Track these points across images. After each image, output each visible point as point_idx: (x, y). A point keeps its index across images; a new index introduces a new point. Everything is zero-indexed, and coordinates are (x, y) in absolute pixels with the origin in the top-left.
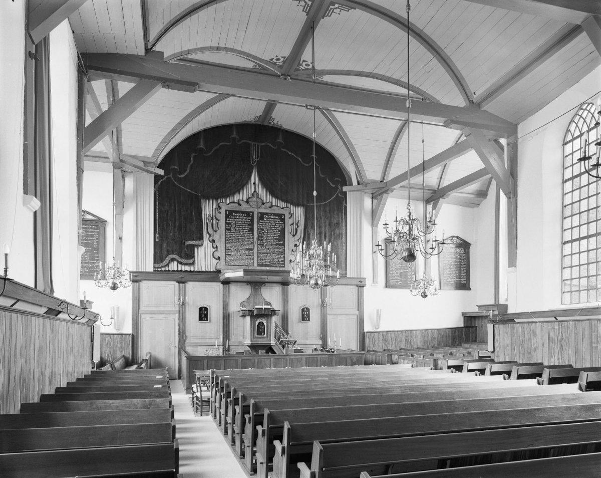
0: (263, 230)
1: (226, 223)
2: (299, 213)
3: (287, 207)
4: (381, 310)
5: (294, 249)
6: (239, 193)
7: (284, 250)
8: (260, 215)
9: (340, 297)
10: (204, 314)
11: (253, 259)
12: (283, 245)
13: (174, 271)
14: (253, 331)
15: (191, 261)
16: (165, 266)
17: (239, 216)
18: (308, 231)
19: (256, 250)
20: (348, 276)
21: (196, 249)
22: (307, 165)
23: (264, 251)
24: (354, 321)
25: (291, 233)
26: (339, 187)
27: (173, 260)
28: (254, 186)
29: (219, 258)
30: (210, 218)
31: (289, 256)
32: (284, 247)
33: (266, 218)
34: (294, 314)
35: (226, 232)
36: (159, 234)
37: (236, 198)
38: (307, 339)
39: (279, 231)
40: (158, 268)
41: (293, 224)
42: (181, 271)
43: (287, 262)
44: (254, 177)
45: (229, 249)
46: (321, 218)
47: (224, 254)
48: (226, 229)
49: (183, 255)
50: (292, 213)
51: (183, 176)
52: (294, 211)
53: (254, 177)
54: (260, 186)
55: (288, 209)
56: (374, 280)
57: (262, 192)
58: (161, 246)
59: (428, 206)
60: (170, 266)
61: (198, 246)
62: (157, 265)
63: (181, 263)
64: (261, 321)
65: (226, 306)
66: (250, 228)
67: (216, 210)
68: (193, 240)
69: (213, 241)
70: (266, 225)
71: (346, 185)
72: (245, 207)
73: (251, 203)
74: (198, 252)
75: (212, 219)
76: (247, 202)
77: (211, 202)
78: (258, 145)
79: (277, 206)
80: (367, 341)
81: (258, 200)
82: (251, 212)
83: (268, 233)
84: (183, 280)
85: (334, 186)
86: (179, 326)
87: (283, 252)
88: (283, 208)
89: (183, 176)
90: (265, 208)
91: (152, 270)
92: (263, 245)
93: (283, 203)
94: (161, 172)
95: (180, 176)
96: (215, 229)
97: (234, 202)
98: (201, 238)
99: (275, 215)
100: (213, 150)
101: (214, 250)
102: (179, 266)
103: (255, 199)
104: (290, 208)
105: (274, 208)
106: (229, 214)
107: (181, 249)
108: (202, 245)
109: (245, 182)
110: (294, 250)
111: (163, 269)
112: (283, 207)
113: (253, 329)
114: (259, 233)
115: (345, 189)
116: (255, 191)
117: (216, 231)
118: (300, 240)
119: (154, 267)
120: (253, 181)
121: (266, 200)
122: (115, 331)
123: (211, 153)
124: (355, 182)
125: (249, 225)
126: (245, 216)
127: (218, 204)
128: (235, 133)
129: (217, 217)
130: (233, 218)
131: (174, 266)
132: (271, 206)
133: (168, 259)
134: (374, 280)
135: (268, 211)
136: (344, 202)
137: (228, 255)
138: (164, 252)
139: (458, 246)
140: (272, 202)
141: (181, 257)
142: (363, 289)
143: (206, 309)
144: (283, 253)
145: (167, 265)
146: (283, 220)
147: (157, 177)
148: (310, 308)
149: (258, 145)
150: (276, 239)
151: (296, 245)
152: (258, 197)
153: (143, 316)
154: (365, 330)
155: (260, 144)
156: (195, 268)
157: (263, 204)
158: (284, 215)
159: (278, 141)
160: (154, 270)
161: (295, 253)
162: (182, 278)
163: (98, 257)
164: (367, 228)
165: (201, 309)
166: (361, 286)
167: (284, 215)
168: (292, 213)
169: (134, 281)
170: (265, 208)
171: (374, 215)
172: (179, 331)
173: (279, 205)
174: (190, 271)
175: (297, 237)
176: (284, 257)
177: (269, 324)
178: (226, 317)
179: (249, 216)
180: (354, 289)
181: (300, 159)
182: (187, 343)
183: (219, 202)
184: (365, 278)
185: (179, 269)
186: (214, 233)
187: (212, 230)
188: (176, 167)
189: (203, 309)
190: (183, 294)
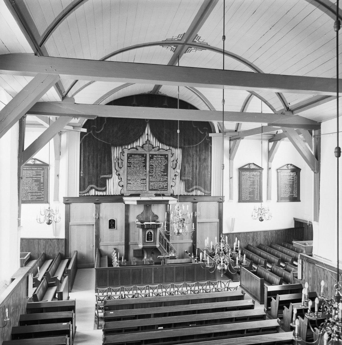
1: (128, 162)
2: (178, 152)
3: (170, 149)
4: (234, 219)
5: (174, 178)
6: (137, 142)
7: (167, 179)
8: (151, 156)
9: (207, 210)
10: (112, 224)
11: (146, 186)
12: (167, 175)
13: (92, 196)
15: (104, 189)
16: (86, 193)
17: (137, 157)
18: (184, 165)
19: (148, 180)
20: (212, 195)
21: (107, 181)
23: (154, 180)
27: (92, 188)
29: (123, 186)
30: (117, 159)
31: (170, 183)
32: (167, 177)
33: (155, 158)
35: (127, 168)
36: (83, 171)
37: (135, 145)
40: (82, 194)
41: (174, 161)
42: (97, 195)
43: (169, 187)
44: (148, 130)
45: (129, 180)
46: (193, 156)
47: (126, 183)
48: (128, 166)
49: (99, 185)
50: (173, 153)
51: (100, 132)
55: (170, 151)
56: (231, 197)
57: (153, 140)
58: (84, 179)
59: (270, 143)
60: (90, 192)
61: (109, 178)
62: (81, 192)
63: (97, 190)
67: (121, 155)
68: (105, 174)
69: (119, 175)
70: (155, 162)
71: (211, 132)
72: (141, 151)
73: (144, 148)
74: (109, 183)
75: (118, 159)
76: (142, 147)
77: (118, 148)
79: (163, 149)
81: (150, 146)
82: (145, 154)
83: (156, 167)
85: (202, 133)
86: (96, 233)
88: (167, 150)
89: (100, 132)
90: (154, 151)
91: (78, 196)
92: (152, 176)
93: (167, 147)
94: (85, 130)
95: (97, 132)
96: (120, 166)
97: (133, 148)
98: (111, 173)
99: (161, 155)
101: (119, 180)
102: (96, 192)
103: (147, 145)
104: (172, 150)
105: (161, 150)
106: (130, 156)
107: (97, 181)
108: (111, 178)
109: (141, 134)
111: (86, 195)
112: (167, 149)
114: (150, 167)
115: (210, 135)
116: (148, 140)
117: (121, 168)
119: (80, 194)
121: (156, 145)
125: (143, 163)
126: (140, 157)
127: (123, 150)
129: (121, 158)
130: (132, 159)
131: (92, 192)
132: (159, 149)
133: (89, 188)
134: (231, 197)
135: (157, 153)
136: (210, 144)
137: (129, 183)
138: (86, 183)
139: (293, 171)
140: (159, 147)
141: (97, 186)
143: (114, 221)
144: (167, 181)
145: (88, 192)
146: (167, 159)
147: (82, 134)
150: (162, 172)
151: (175, 175)
153: (72, 227)
156: (106, 193)
157: (153, 148)
158: (168, 155)
160: (80, 196)
161: (175, 180)
163: (43, 188)
165: (110, 221)
166: (221, 201)
167: (168, 155)
168: (173, 153)
169: (66, 204)
170: (155, 151)
171: (231, 151)
172: (96, 236)
173: (164, 148)
174: (103, 196)
176: (167, 183)
178: (127, 226)
180: (216, 204)
182: (101, 244)
183: (123, 148)
185: (96, 194)
186: (120, 169)
187: (118, 167)
188: (95, 126)
189: (112, 221)
190: (98, 211)
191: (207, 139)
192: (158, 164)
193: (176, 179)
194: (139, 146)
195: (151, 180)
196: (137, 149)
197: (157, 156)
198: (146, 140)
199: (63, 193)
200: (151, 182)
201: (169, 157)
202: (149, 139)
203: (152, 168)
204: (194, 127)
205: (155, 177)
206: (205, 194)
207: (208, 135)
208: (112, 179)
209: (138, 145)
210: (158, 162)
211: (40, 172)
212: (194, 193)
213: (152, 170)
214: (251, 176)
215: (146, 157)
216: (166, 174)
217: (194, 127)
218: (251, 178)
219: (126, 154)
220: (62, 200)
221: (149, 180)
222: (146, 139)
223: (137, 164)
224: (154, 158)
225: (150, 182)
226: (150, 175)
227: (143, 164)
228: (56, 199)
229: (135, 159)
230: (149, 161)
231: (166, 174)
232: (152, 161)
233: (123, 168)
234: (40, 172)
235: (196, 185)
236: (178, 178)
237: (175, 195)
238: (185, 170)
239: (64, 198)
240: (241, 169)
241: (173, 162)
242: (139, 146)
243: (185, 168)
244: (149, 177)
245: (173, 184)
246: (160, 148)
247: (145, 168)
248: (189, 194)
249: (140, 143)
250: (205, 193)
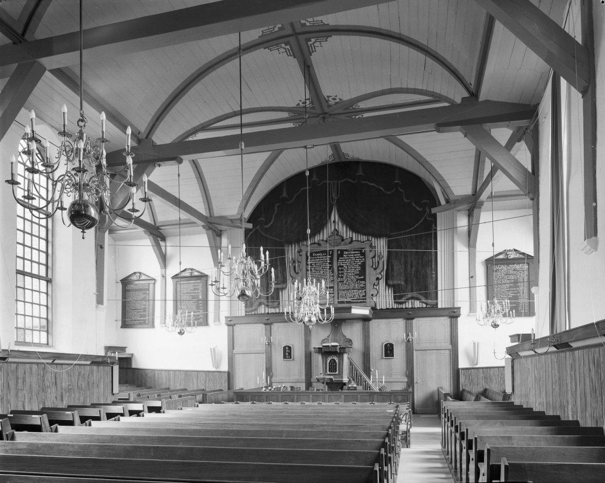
0: (342, 266)
2: (381, 245)
4: (478, 343)
5: (376, 282)
6: (320, 234)
8: (339, 252)
10: (288, 353)
12: (364, 279)
13: (261, 314)
14: (341, 368)
18: (392, 262)
20: (439, 306)
22: (389, 193)
23: (345, 287)
24: (446, 356)
25: (372, 266)
26: (428, 210)
27: (260, 304)
28: (335, 223)
31: (370, 290)
33: (346, 254)
34: (376, 351)
38: (391, 376)
39: (360, 265)
41: (374, 257)
44: (334, 216)
52: (376, 244)
53: (334, 216)
54: (340, 224)
56: (472, 309)
61: (283, 289)
64: (332, 358)
65: (307, 343)
70: (346, 261)
74: (282, 295)
75: (294, 262)
77: (294, 247)
78: (338, 183)
80: (462, 379)
84: (269, 322)
87: (364, 287)
88: (363, 242)
90: (344, 245)
92: (343, 282)
93: (364, 237)
95: (265, 227)
97: (315, 243)
100: (295, 197)
102: (267, 309)
108: (286, 288)
110: (376, 284)
111: (253, 313)
113: (324, 366)
114: (338, 270)
115: (434, 210)
117: (297, 273)
118: (382, 273)
119: (246, 312)
120: (332, 219)
121: (347, 236)
122: (214, 369)
123: (292, 201)
124: (443, 202)
126: (325, 256)
128: (315, 176)
134: (472, 309)
135: (347, 247)
136: (433, 226)
140: (352, 238)
142: (457, 320)
143: (290, 348)
144: (364, 288)
145: (256, 309)
147: (247, 231)
148: (394, 344)
149: (338, 183)
150: (356, 275)
151: (378, 279)
152: (337, 234)
153: (237, 356)
154: (460, 366)
155: (340, 181)
156: (279, 310)
160: (246, 315)
162: (268, 319)
164: (461, 252)
165: (285, 348)
166: (453, 314)
168: (373, 245)
172: (266, 368)
173: (359, 240)
174: (276, 313)
175: (378, 271)
176: (365, 292)
177: (341, 363)
183: (301, 245)
184: (460, 308)
186: (296, 275)
187: (295, 274)
189: (287, 348)
190: (269, 334)
191: (428, 218)
192: (350, 263)
193: (378, 283)
194: (323, 240)
196: (319, 244)
198: (332, 231)
199: (225, 312)
201: (367, 253)
202: (337, 228)
203: (342, 270)
204: (406, 201)
205: (346, 283)
206: (428, 306)
207: (430, 211)
208: (286, 291)
209: (321, 238)
210: (350, 260)
211: (197, 286)
212: (409, 305)
213: (342, 274)
214: (511, 272)
215: (332, 255)
216: (362, 277)
217: (406, 201)
218: (510, 274)
219: (303, 253)
220: (223, 320)
221: (338, 288)
222: (333, 228)
223: (320, 265)
224: (344, 256)
228: (217, 319)
229: (317, 259)
230: (338, 261)
231: (362, 277)
233: (300, 274)
234: (197, 286)
235: (412, 291)
236: (382, 283)
237: (378, 308)
238: (393, 269)
239: (226, 317)
240: (490, 263)
241: (374, 259)
242: (323, 240)
243: (392, 266)
245: (375, 292)
246: (354, 239)
248: (400, 306)
249: (325, 234)
250: (427, 304)
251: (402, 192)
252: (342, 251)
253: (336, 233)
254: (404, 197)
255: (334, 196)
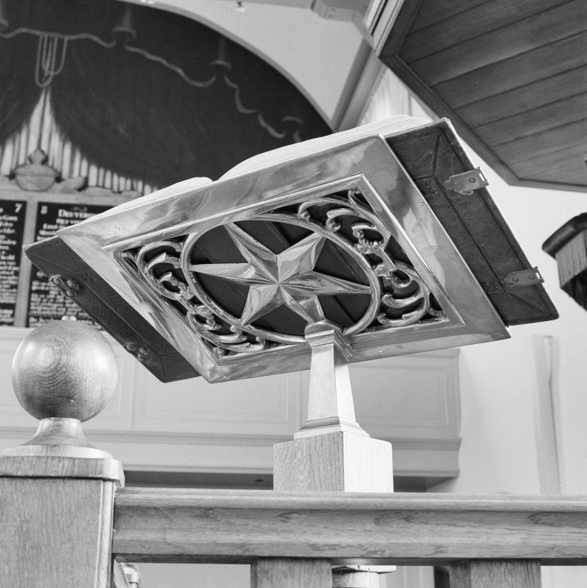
8: (44, 210)
22: (199, 85)
33: (64, 218)
54: (56, 141)
57: (60, 152)
66: (10, 246)
73: (19, 178)
78: (61, 42)
82: (19, 202)
92: (46, 293)
93: (122, 180)
121: (71, 171)
125: (9, 237)
135: (72, 199)
140: (86, 180)
149: (61, 42)
152: (45, 161)
155: (67, 38)
157: (59, 179)
159: (120, 29)
179: (12, 213)
181: (180, 71)
195: (37, 309)
197: (73, 211)
200: (37, 317)
202: (44, 147)
204: (242, 109)
205: (55, 299)
215: (22, 215)
221: (29, 310)
224: (58, 221)
225: (32, 320)
226: (34, 288)
227: (9, 242)
232: (47, 230)
244: (30, 297)
246: (92, 182)
247: (12, 257)
251: (234, 90)
252: (54, 208)
253: (40, 157)
254: (238, 101)
255: (46, 67)
